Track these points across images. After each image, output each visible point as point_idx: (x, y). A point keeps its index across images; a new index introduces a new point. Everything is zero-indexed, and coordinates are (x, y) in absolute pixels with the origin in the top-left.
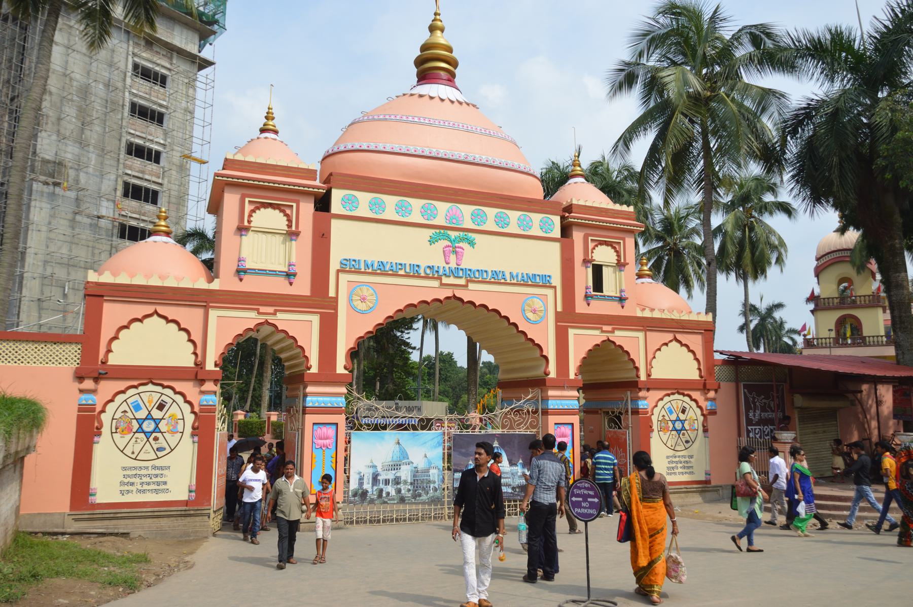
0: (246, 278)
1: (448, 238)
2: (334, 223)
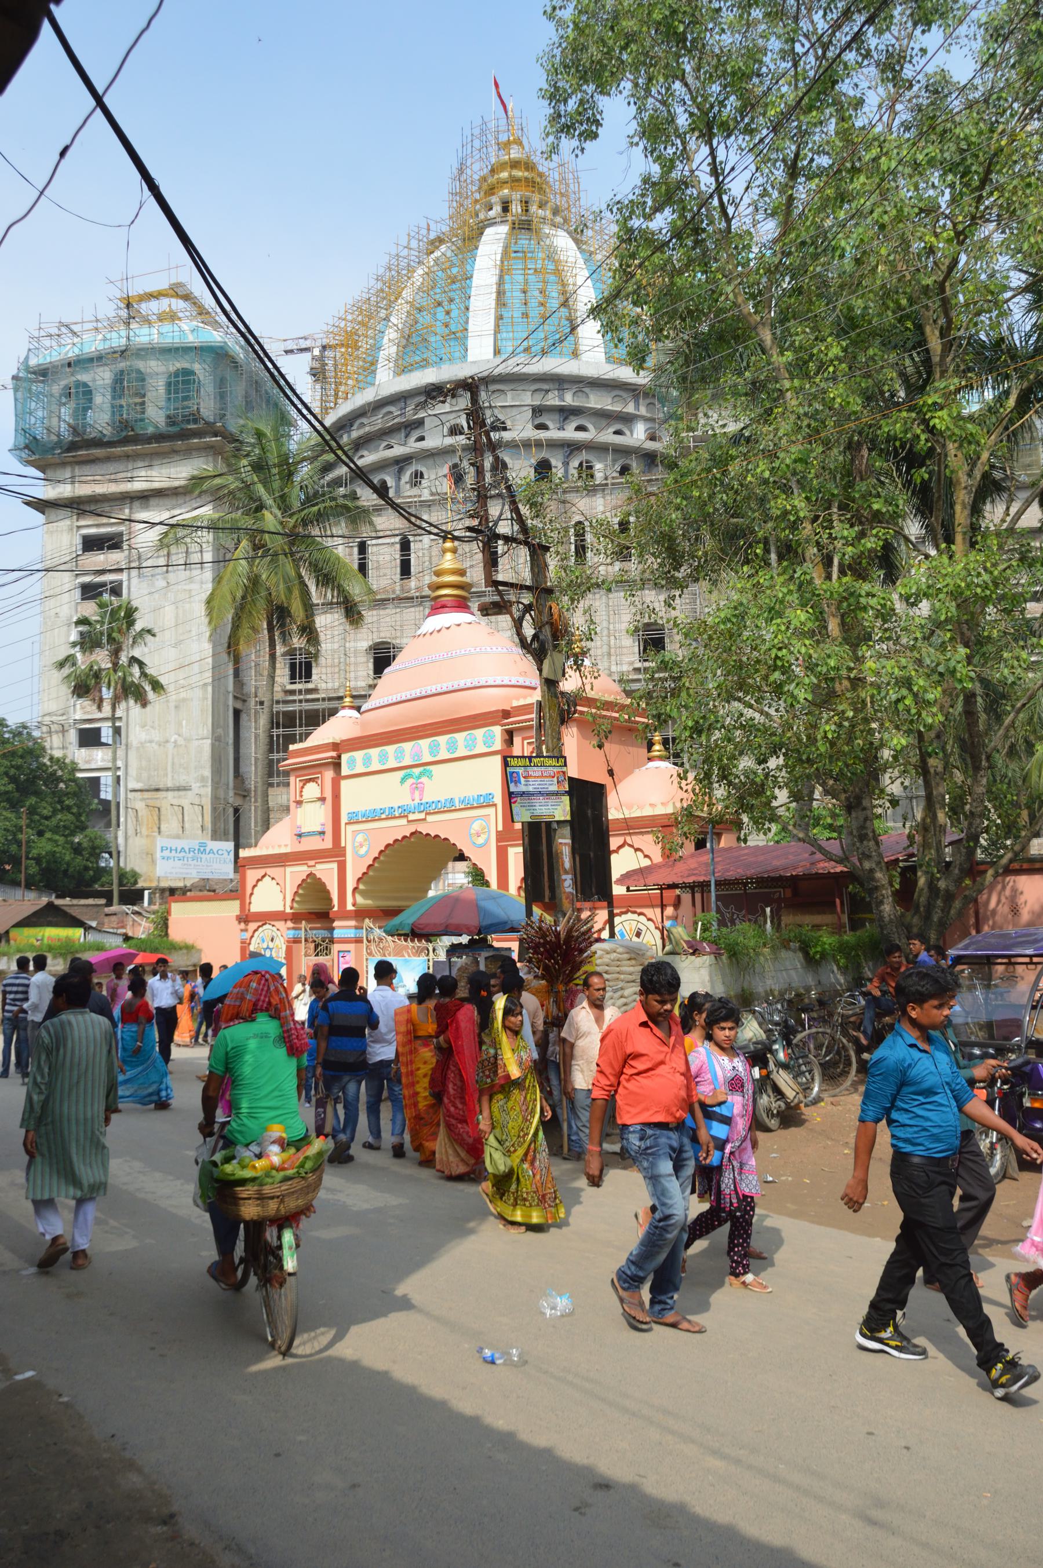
0: (303, 839)
1: (410, 776)
2: (344, 784)
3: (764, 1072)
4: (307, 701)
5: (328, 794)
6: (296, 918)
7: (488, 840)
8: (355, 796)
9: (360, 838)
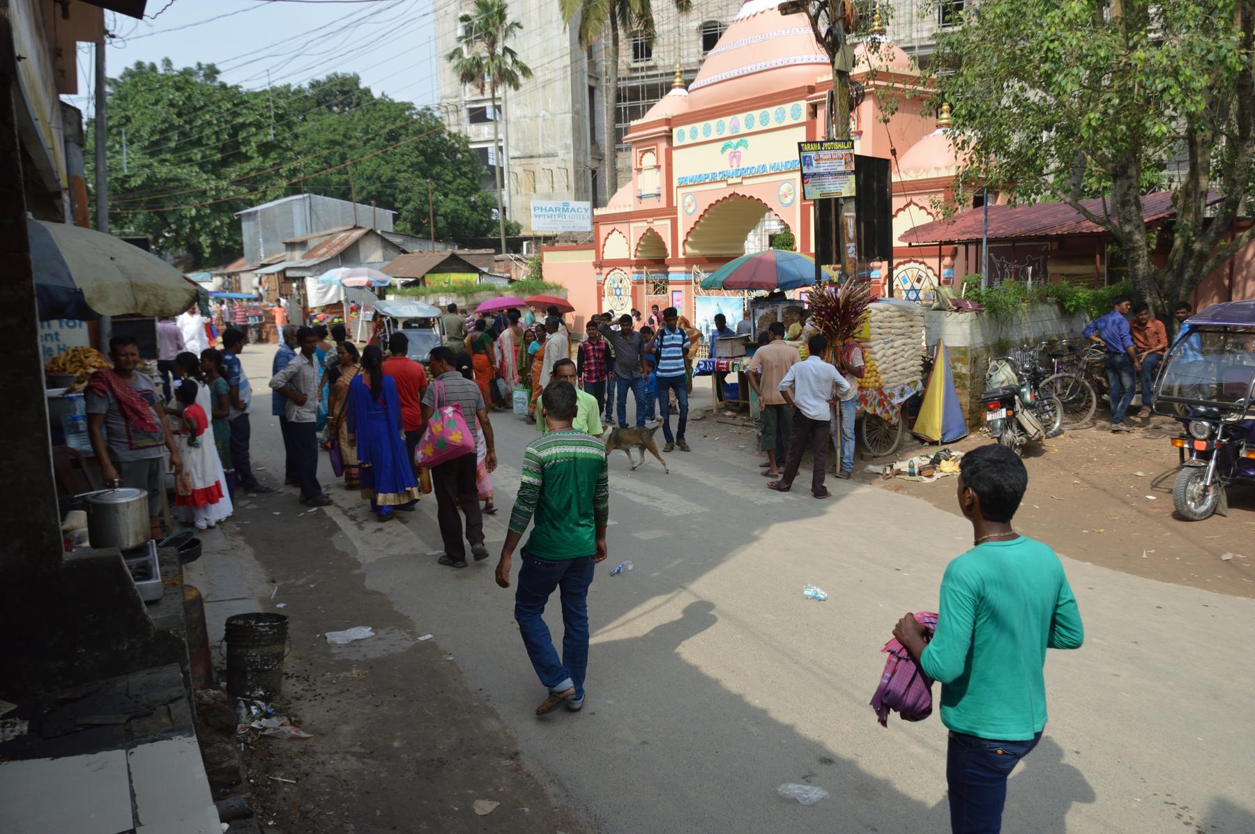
2: (675, 154)
3: (1011, 412)
4: (648, 77)
5: (663, 163)
6: (639, 264)
7: (793, 201)
8: (685, 163)
9: (688, 199)
